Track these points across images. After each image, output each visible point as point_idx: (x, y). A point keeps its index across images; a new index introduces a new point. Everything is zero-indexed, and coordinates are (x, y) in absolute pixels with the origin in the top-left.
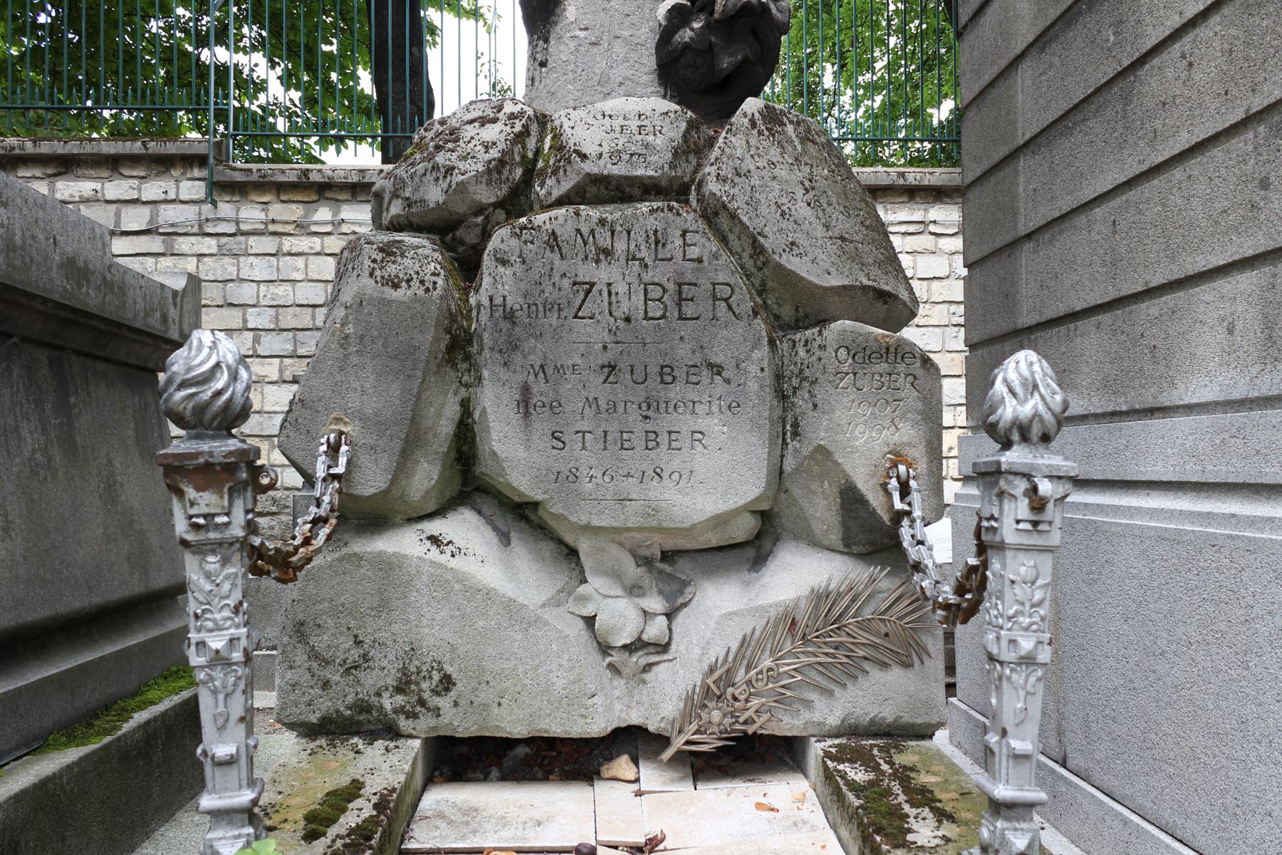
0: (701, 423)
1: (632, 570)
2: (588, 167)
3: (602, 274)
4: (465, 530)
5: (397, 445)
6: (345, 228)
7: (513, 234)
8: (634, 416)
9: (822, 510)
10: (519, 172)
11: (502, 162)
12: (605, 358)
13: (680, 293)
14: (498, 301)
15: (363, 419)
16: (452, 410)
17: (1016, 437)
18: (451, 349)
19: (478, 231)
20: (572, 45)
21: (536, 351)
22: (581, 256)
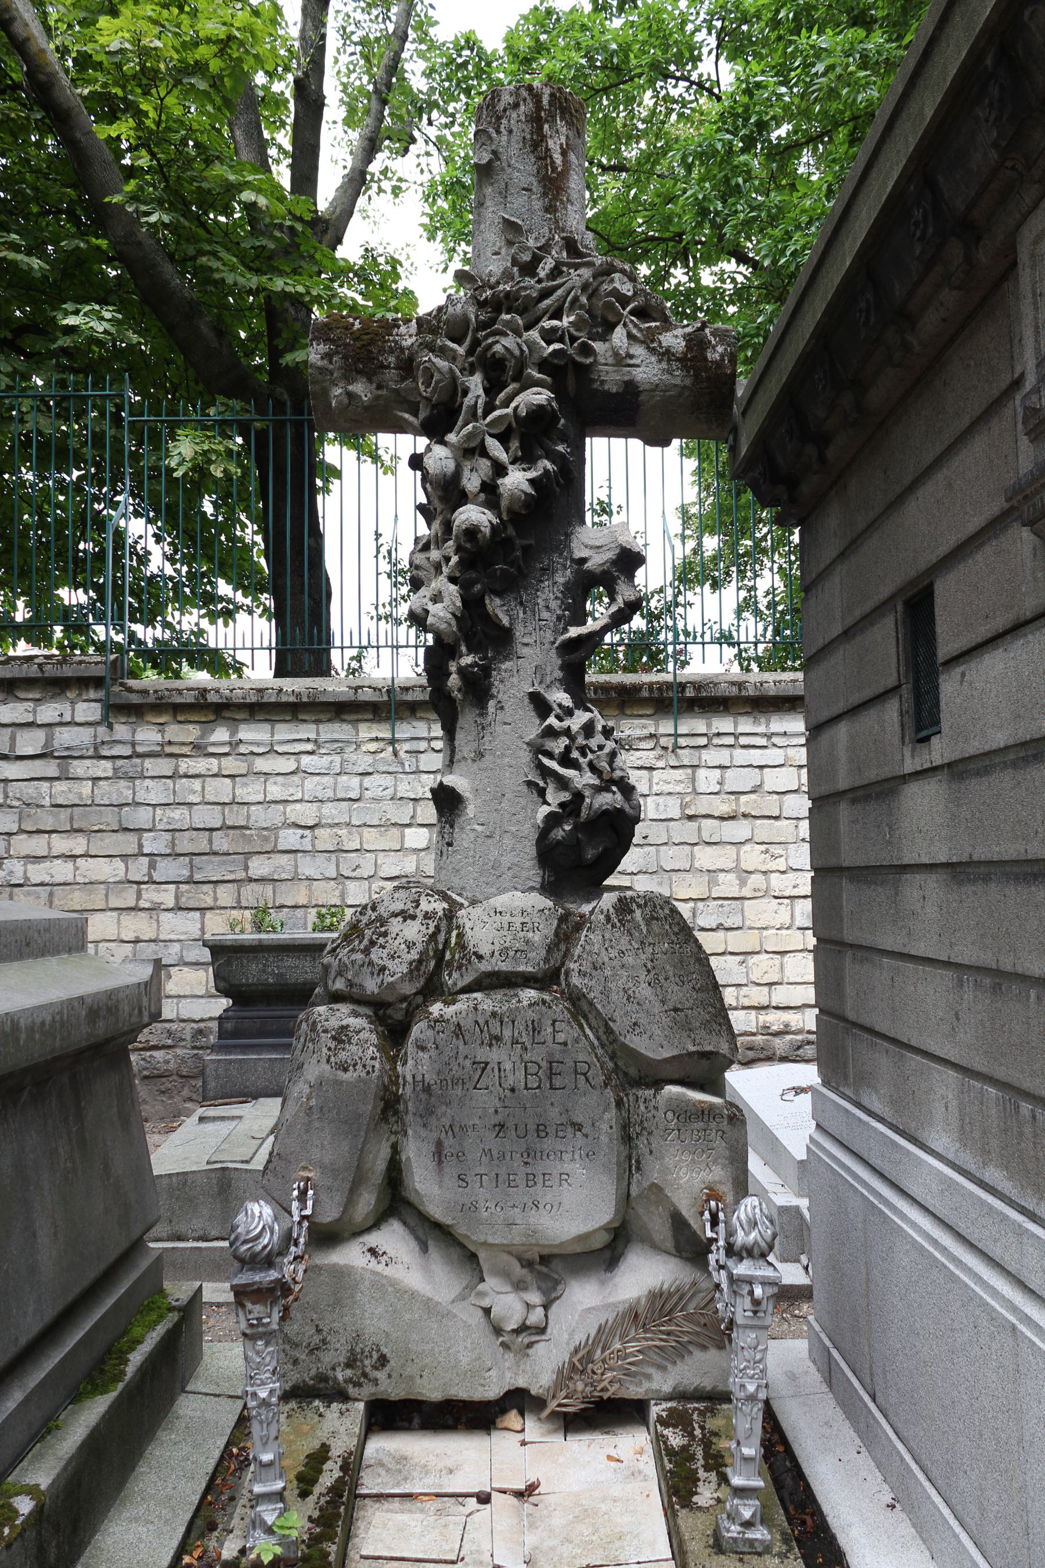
0: (567, 1167)
1: (518, 1271)
2: (484, 967)
3: (495, 1055)
4: (393, 1239)
5: (347, 1186)
6: (243, 749)
7: (430, 1026)
8: (517, 1163)
9: (659, 1227)
10: (432, 963)
11: (420, 962)
12: (496, 1120)
13: (551, 1069)
14: (419, 1078)
15: (323, 1167)
16: (385, 1152)
17: (745, 1254)
18: (384, 1111)
19: (403, 1012)
20: (472, 835)
21: (447, 1114)
22: (479, 1042)
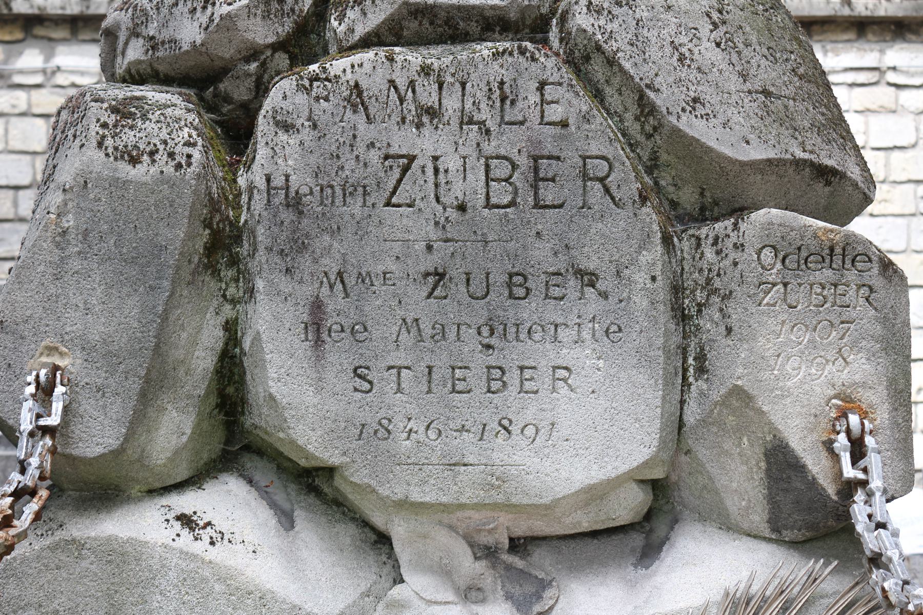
0: (567, 356)
1: (468, 565)
3: (425, 143)
4: (228, 503)
5: (135, 385)
6: (60, 79)
7: (300, 88)
9: (739, 480)
12: (429, 263)
13: (536, 170)
14: (279, 181)
15: (87, 348)
16: (212, 336)
18: (212, 249)
19: (250, 83)
21: (332, 251)
22: (396, 118)
